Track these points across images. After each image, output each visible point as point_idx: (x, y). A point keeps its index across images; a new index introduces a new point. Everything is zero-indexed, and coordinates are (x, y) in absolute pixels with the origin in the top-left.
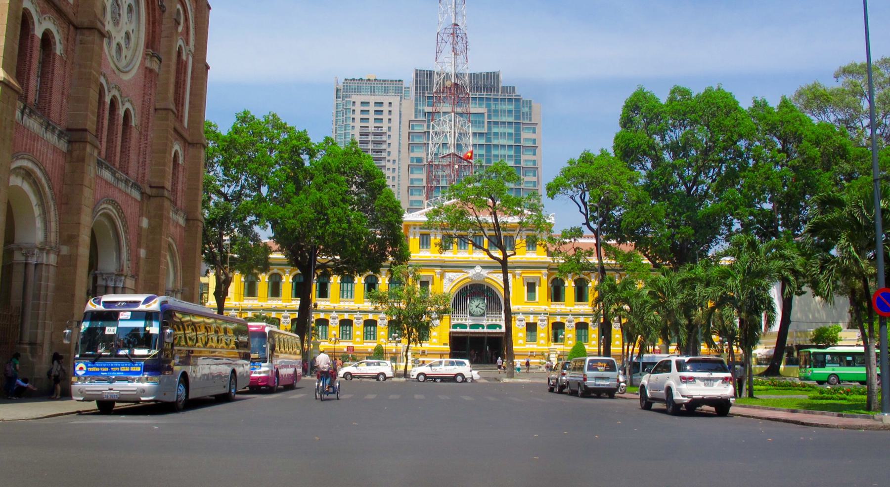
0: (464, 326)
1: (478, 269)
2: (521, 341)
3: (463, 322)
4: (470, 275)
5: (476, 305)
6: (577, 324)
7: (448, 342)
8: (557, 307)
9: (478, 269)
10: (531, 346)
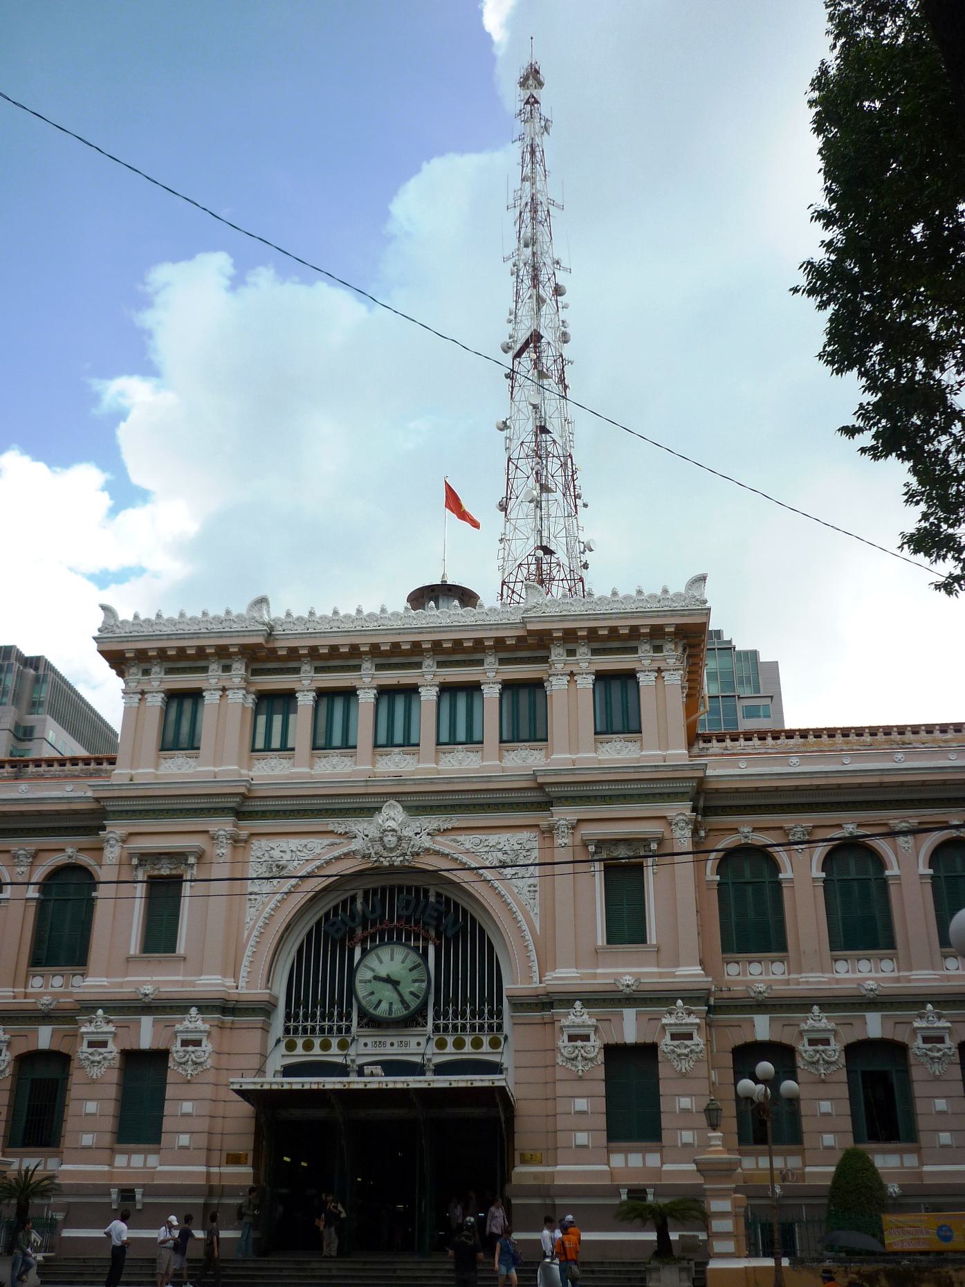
0: (342, 1070)
1: (392, 816)
2: (582, 1138)
3: (334, 1055)
4: (356, 845)
6: (854, 1050)
7: (245, 1144)
8: (758, 975)
9: (392, 816)
10: (635, 1160)
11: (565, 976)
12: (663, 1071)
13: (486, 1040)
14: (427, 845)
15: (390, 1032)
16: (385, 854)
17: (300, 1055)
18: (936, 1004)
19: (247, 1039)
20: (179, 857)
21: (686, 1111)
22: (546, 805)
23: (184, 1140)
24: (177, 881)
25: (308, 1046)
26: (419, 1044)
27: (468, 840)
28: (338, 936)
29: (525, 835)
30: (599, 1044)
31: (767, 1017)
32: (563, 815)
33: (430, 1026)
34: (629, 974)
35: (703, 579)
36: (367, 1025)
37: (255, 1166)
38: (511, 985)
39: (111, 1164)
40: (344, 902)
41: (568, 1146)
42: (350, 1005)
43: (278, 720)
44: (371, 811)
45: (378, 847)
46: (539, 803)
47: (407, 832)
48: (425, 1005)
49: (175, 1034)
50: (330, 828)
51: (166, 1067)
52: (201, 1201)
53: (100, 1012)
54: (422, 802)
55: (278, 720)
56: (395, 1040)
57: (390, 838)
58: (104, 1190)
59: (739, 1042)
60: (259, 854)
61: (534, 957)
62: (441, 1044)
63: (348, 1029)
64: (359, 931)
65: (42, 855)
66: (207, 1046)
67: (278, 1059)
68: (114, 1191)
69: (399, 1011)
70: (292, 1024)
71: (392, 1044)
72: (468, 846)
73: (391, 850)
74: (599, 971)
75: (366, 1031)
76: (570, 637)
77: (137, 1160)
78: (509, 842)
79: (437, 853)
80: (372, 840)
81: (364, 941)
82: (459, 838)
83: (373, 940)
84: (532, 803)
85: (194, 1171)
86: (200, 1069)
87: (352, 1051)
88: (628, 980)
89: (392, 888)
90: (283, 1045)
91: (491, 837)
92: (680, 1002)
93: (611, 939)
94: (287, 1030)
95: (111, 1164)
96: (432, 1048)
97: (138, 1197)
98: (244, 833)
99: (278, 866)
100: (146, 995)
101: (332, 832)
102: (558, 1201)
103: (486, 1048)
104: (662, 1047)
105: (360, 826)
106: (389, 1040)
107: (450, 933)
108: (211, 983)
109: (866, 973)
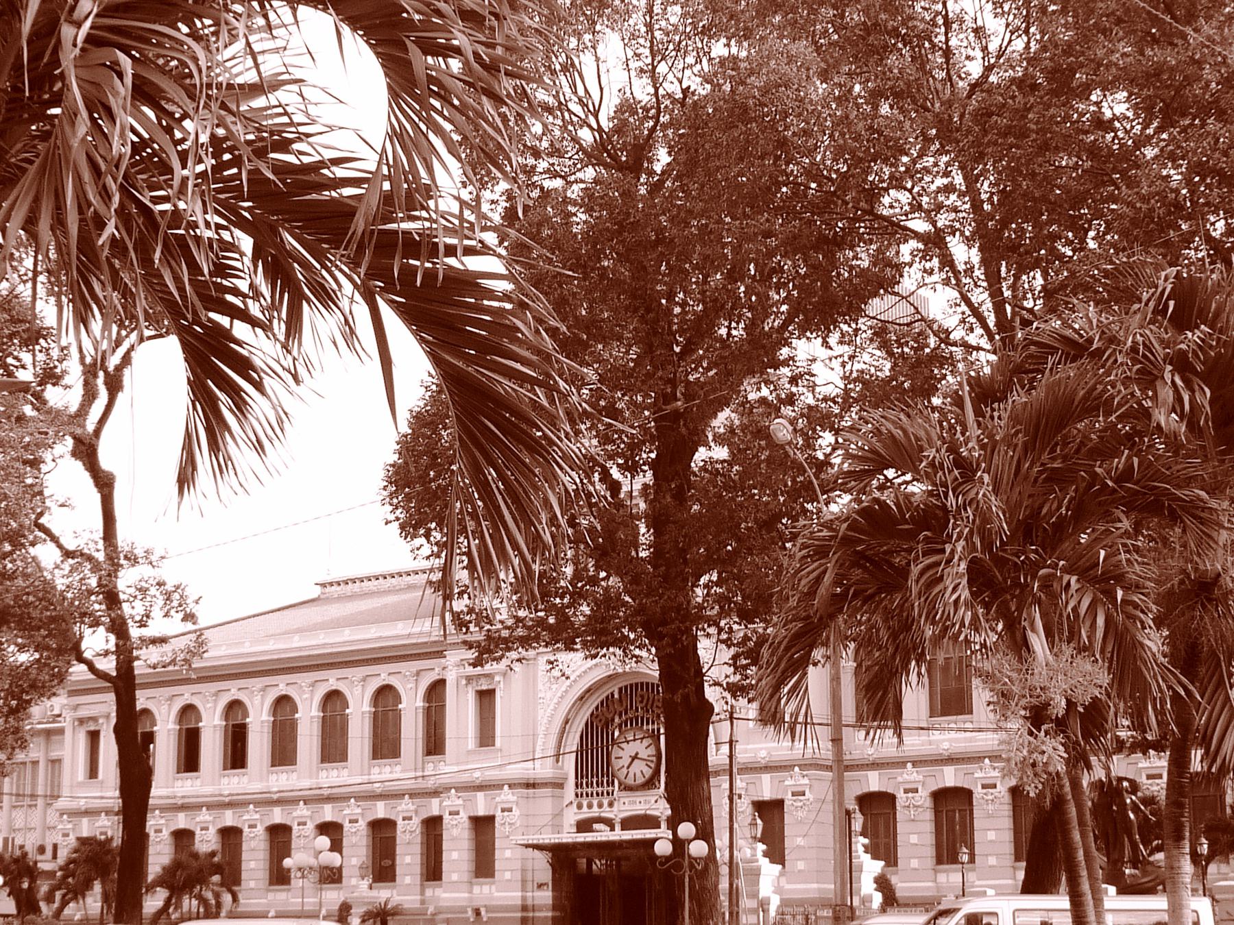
0: (610, 823)
7: (546, 875)
12: (787, 819)
15: (638, 793)
17: (586, 814)
19: (544, 802)
23: (508, 875)
25: (590, 806)
31: (876, 773)
36: (625, 789)
39: (471, 892)
48: (657, 772)
51: (494, 827)
52: (519, 915)
56: (642, 799)
58: (463, 910)
59: (859, 793)
64: (617, 720)
65: (423, 673)
66: (516, 812)
67: (572, 816)
68: (469, 910)
69: (641, 780)
70: (579, 790)
75: (624, 793)
77: (486, 889)
85: (513, 896)
87: (615, 808)
88: (763, 754)
89: (637, 684)
90: (575, 805)
92: (797, 769)
94: (577, 795)
95: (471, 892)
97: (483, 913)
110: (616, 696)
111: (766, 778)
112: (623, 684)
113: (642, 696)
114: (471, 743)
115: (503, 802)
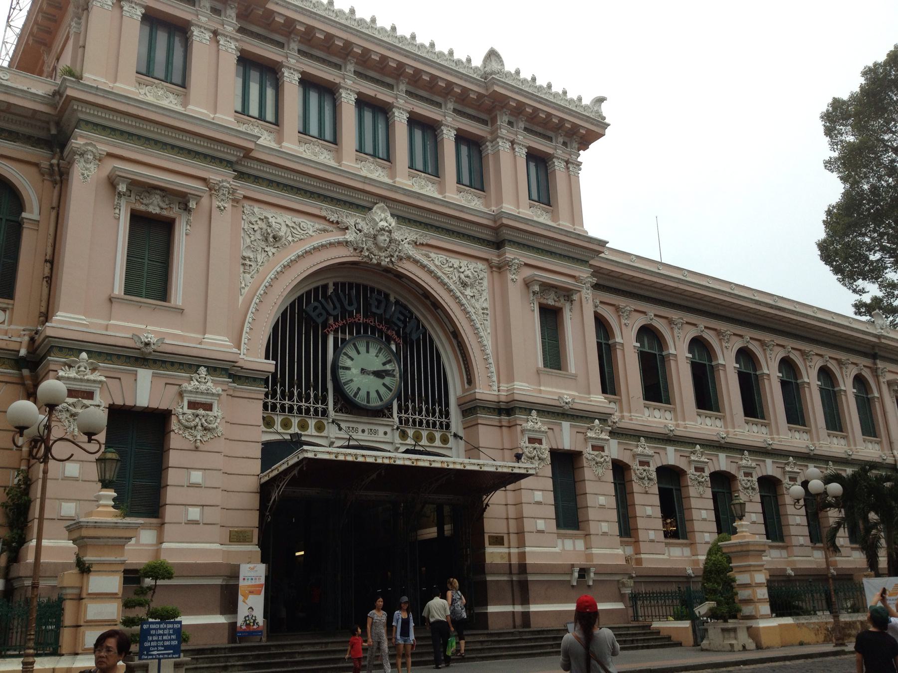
2: (541, 525)
4: (350, 236)
5: (363, 367)
7: (251, 520)
9: (383, 217)
11: (524, 388)
13: (438, 435)
14: (411, 253)
16: (376, 252)
18: (702, 445)
20: (182, 200)
21: (602, 507)
22: (498, 245)
23: (194, 513)
24: (167, 226)
25: (286, 425)
26: (385, 433)
27: (438, 258)
28: (320, 321)
29: (481, 266)
30: (548, 447)
31: (616, 441)
32: (511, 254)
33: (396, 420)
34: (568, 395)
35: (601, 100)
36: (341, 410)
37: (261, 544)
38: (455, 389)
40: (316, 289)
41: (526, 529)
42: (325, 389)
43: (254, 89)
44: (365, 209)
45: (370, 243)
46: (489, 241)
47: (397, 235)
49: (181, 394)
50: (324, 213)
53: (84, 355)
54: (413, 215)
55: (254, 89)
56: (366, 427)
57: (382, 238)
60: (253, 220)
61: (493, 369)
62: (404, 435)
63: (325, 413)
64: (331, 321)
69: (375, 403)
71: (363, 431)
72: (437, 262)
73: (380, 249)
74: (542, 388)
76: (518, 111)
78: (470, 268)
79: (416, 262)
80: (366, 235)
81: (336, 331)
82: (432, 255)
83: (344, 332)
84: (484, 240)
86: (209, 435)
91: (453, 261)
93: (545, 365)
94: (265, 406)
96: (398, 440)
98: (241, 192)
99: (274, 237)
100: (147, 344)
101: (324, 218)
102: (530, 578)
103: (438, 443)
104: (586, 455)
105: (351, 219)
106: (361, 427)
107: (414, 337)
108: (217, 343)
109: (655, 418)
110: (331, 290)
111: (566, 425)
112: (338, 280)
113: (379, 302)
114: (118, 289)
115: (196, 392)
